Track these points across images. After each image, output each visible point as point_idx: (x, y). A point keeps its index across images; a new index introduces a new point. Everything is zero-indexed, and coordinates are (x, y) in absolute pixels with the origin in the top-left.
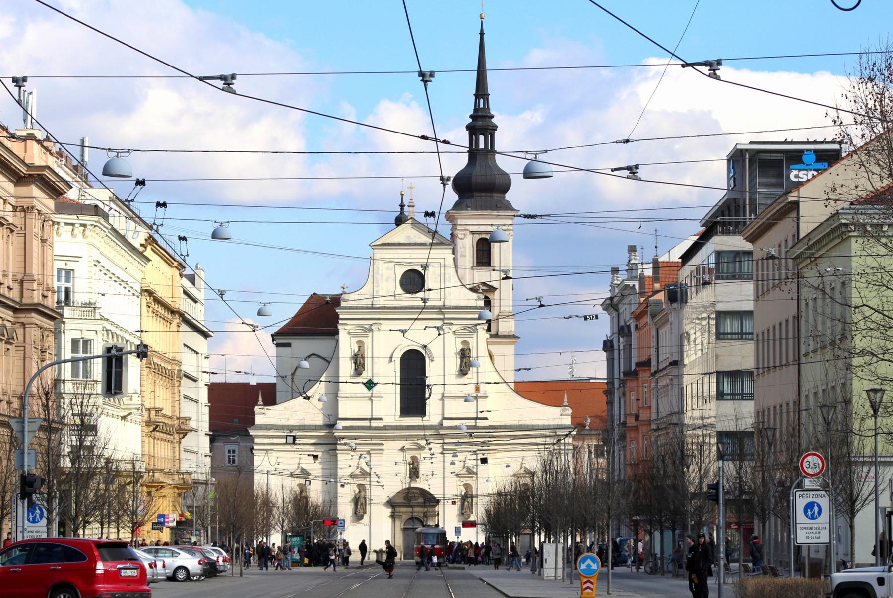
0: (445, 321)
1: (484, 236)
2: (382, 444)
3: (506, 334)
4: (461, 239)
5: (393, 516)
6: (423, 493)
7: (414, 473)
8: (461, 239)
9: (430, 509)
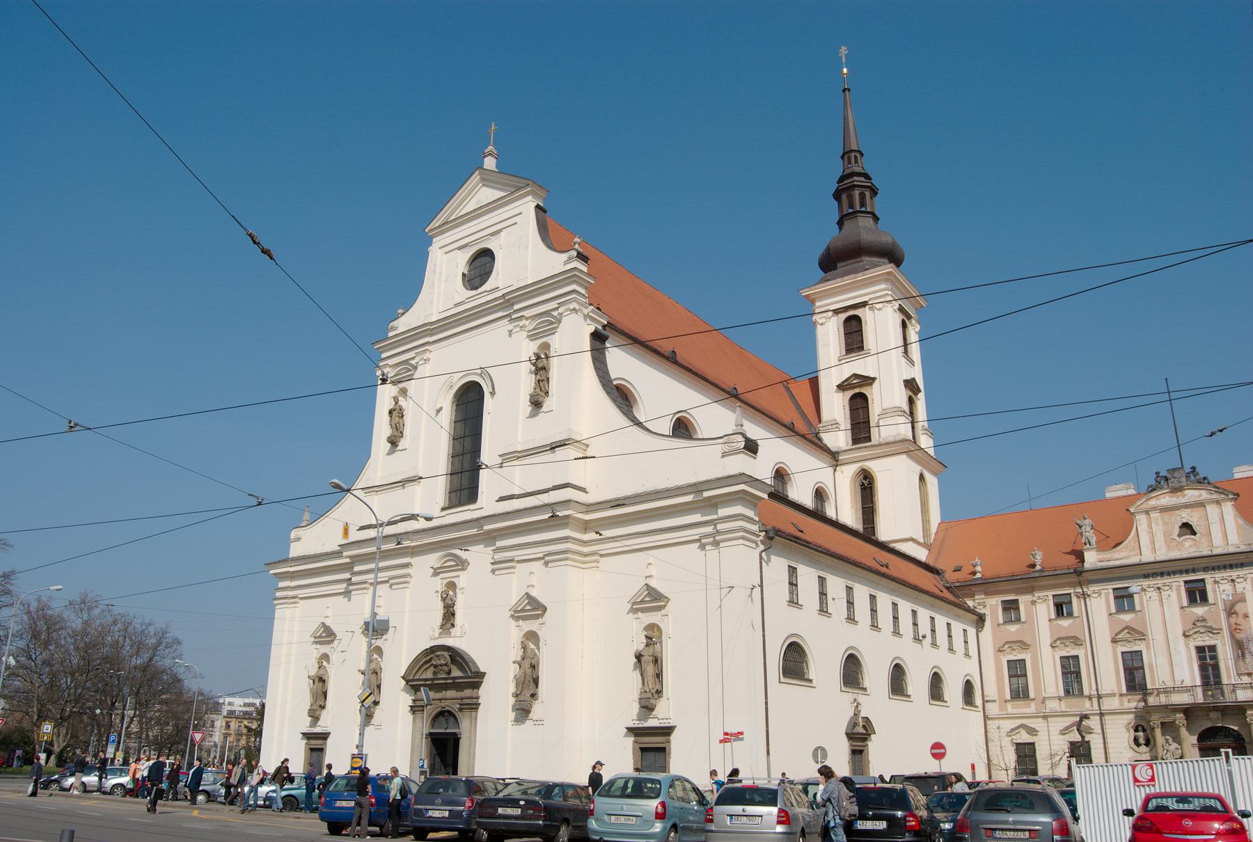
0: (513, 317)
1: (851, 313)
2: (407, 565)
3: (891, 439)
4: (822, 324)
5: (414, 709)
6: (457, 657)
7: (449, 615)
8: (822, 324)
9: (467, 692)
